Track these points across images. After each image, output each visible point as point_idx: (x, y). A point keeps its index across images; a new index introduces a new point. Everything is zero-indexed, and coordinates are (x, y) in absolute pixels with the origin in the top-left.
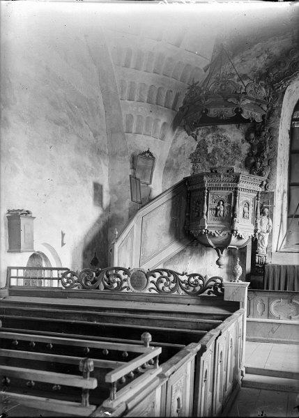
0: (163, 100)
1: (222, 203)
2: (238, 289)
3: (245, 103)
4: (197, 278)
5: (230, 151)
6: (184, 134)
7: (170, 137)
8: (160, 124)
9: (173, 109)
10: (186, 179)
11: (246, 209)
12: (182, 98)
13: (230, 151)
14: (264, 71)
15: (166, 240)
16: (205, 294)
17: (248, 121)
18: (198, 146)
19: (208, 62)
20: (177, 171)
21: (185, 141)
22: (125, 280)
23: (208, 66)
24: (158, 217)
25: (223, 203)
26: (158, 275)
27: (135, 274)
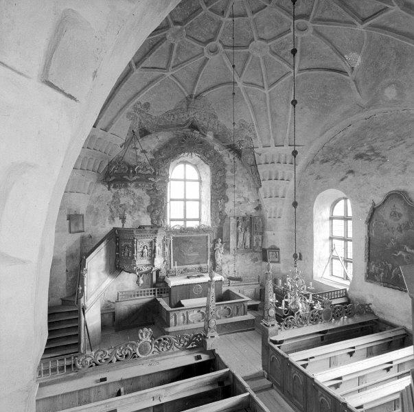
0: (91, 167)
5: (136, 201)
8: (88, 183)
13: (136, 201)
15: (104, 276)
18: (114, 197)
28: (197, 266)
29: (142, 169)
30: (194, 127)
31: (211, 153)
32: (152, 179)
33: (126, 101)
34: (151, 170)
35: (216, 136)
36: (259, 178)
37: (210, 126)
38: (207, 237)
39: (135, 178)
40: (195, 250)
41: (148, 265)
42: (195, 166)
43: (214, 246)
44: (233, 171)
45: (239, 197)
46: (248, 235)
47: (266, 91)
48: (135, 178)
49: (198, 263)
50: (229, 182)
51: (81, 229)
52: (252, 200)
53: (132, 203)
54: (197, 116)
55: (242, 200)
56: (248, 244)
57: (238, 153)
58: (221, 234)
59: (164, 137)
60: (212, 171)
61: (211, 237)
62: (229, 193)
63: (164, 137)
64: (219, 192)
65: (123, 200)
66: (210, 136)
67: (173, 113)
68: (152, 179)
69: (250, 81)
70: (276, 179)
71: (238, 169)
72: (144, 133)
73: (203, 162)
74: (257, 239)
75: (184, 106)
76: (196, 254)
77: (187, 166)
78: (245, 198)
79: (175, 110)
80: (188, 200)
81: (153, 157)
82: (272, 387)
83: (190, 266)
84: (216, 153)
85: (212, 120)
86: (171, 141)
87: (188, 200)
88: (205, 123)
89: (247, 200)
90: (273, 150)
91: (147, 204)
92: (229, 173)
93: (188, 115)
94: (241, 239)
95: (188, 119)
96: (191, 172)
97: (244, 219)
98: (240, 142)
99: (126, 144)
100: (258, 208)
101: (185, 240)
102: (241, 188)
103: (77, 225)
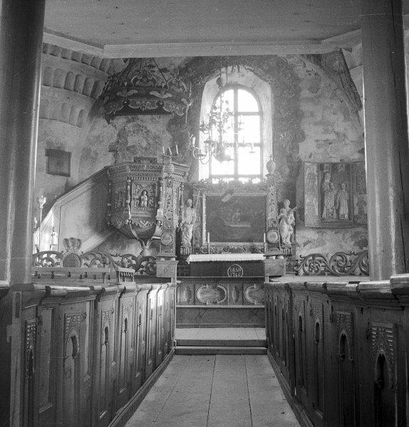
1: (145, 193)
2: (167, 266)
3: (165, 96)
4: (130, 258)
5: (151, 141)
6: (103, 122)
7: (87, 126)
8: (78, 110)
9: (92, 96)
10: (106, 168)
12: (102, 85)
13: (151, 141)
14: (183, 66)
15: (86, 231)
17: (170, 113)
18: (119, 135)
20: (94, 160)
21: (106, 131)
22: (58, 264)
25: (147, 193)
26: (91, 258)
27: (68, 257)
28: (248, 244)
29: (141, 81)
32: (157, 94)
41: (147, 219)
42: (252, 90)
44: (314, 89)
45: (326, 131)
49: (249, 241)
50: (306, 107)
51: (65, 171)
52: (352, 136)
53: (144, 144)
55: (332, 137)
56: (344, 211)
58: (291, 194)
60: (273, 91)
65: (132, 140)
73: (261, 81)
76: (247, 225)
77: (241, 92)
78: (337, 134)
82: (264, 353)
83: (234, 244)
89: (341, 136)
92: (305, 93)
94: (329, 203)
96: (246, 100)
97: (334, 166)
102: (332, 118)
103: (59, 164)
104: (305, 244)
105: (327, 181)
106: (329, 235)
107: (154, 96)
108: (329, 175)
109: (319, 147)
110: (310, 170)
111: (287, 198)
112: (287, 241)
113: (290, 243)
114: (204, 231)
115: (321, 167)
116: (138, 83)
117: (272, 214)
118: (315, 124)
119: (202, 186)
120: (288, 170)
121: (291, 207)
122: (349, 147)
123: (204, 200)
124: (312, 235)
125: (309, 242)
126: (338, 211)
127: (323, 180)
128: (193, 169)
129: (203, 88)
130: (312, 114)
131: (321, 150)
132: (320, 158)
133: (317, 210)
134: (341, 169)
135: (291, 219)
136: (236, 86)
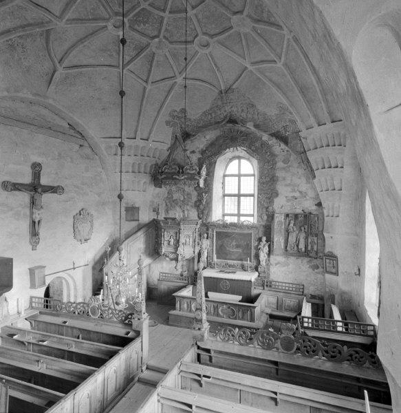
0: (142, 170)
8: (142, 182)
11: (188, 240)
16: (127, 322)
19: (169, 146)
23: (169, 148)
24: (138, 244)
30: (233, 121)
31: (258, 144)
33: (156, 113)
34: (175, 169)
35: (256, 126)
36: (311, 168)
37: (250, 116)
38: (251, 234)
39: (163, 176)
40: (238, 246)
41: (173, 253)
42: (248, 159)
43: (259, 244)
44: (286, 161)
45: (294, 191)
46: (302, 236)
47: (279, 65)
48: (163, 176)
49: (241, 260)
50: (279, 174)
51: (136, 218)
52: (311, 194)
53: (182, 199)
54: (234, 109)
55: (297, 194)
56: (302, 246)
57: (285, 140)
59: (211, 135)
61: (254, 235)
62: (281, 188)
63: (211, 135)
64: (268, 187)
65: (176, 196)
66: (250, 126)
67: (210, 112)
68: (197, 177)
69: (258, 59)
70: (330, 167)
71: (292, 158)
72: (187, 136)
74: (313, 242)
75: (220, 103)
76: (240, 250)
77: (242, 161)
78: (301, 192)
79: (211, 109)
80: (234, 195)
81: (201, 156)
83: (231, 261)
84: (264, 144)
85: (251, 110)
86: (217, 139)
87: (234, 195)
88: (244, 115)
90: (318, 131)
91: (194, 198)
92: (280, 164)
93: (225, 111)
94: (292, 239)
95: (225, 114)
97: (296, 216)
98: (285, 128)
99: (172, 148)
100: (319, 204)
101: (227, 235)
102: (297, 181)
103: (133, 215)
104: (276, 264)
105: (292, 225)
106: (292, 259)
107: (176, 179)
108: (292, 222)
109: (288, 201)
110: (279, 219)
111: (265, 236)
112: (263, 263)
113: (264, 264)
114: (214, 252)
115: (287, 215)
116: (166, 171)
117: (254, 243)
118: (286, 185)
119: (214, 225)
120: (265, 217)
121: (267, 241)
122: (308, 202)
123: (215, 234)
124: (281, 259)
125: (279, 263)
126: (298, 246)
127: (289, 224)
128: (209, 214)
129: (215, 163)
130: (284, 179)
131: (289, 204)
132: (287, 210)
133: (283, 245)
134: (301, 219)
135: (266, 249)
136: (239, 158)
